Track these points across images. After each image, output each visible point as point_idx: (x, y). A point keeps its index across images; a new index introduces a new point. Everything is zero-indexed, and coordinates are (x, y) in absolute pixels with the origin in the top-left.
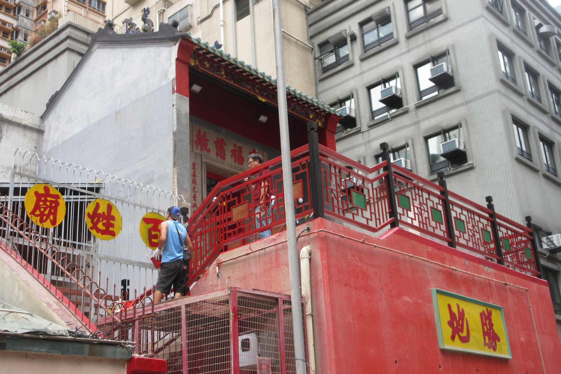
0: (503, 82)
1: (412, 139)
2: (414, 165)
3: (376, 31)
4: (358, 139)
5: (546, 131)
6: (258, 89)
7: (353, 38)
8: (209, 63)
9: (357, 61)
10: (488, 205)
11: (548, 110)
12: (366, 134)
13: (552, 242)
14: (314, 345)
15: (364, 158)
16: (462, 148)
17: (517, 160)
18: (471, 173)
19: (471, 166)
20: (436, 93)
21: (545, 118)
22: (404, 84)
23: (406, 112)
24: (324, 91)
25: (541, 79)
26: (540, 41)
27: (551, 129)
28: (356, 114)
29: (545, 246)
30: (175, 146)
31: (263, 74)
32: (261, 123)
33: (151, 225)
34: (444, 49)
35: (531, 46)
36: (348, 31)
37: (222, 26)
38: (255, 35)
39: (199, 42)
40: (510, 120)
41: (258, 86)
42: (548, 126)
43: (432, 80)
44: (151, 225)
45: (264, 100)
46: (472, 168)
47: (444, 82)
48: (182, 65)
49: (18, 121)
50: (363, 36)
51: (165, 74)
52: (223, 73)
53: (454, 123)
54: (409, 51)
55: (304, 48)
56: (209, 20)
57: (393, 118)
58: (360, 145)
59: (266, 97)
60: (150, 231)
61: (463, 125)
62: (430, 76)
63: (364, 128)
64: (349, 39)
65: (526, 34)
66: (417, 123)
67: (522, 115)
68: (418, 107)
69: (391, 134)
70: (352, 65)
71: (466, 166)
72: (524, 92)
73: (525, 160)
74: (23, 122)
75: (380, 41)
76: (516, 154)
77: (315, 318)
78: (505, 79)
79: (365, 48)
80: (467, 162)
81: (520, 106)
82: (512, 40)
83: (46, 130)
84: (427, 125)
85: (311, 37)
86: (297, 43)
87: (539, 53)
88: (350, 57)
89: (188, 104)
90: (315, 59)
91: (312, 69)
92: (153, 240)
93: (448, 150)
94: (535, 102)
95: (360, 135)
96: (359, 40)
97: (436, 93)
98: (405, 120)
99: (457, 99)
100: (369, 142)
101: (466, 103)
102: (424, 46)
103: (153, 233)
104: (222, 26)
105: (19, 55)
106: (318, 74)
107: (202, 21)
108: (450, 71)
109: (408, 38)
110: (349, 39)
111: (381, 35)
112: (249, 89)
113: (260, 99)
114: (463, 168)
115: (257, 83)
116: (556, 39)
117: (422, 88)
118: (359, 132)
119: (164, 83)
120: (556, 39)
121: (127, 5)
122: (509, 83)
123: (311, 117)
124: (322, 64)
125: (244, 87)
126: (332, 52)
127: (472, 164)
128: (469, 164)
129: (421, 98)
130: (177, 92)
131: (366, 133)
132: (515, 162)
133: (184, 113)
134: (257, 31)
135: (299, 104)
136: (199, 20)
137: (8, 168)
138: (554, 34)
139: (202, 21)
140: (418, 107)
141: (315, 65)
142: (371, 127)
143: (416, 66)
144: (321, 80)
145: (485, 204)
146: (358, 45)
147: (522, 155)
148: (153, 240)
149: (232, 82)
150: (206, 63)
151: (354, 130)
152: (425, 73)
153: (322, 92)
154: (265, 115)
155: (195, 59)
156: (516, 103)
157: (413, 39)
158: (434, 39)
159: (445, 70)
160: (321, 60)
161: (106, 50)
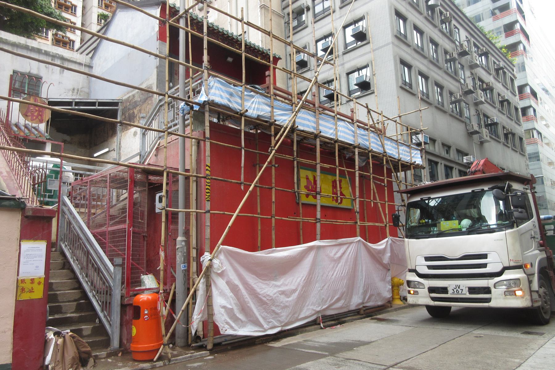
0: (396, 36)
3: (322, 4)
5: (424, 69)
7: (308, 9)
9: (310, 25)
11: (427, 56)
13: (418, 139)
14: (197, 200)
16: (368, 80)
17: (401, 87)
18: (373, 95)
20: (355, 45)
21: (425, 62)
25: (425, 35)
26: (428, 10)
27: (428, 68)
29: (414, 141)
30: (158, 75)
31: (223, 29)
32: (229, 62)
34: (362, 16)
35: (421, 13)
36: (305, 4)
38: (248, 7)
39: (175, 6)
40: (398, 62)
41: (220, 37)
42: (426, 66)
43: (352, 36)
46: (373, 93)
47: (361, 37)
49: (75, 60)
50: (314, 7)
51: (153, 28)
53: (364, 64)
54: (341, 17)
55: (279, 15)
61: (370, 65)
62: (352, 34)
64: (305, 10)
65: (418, 6)
66: (343, 64)
67: (408, 59)
68: (344, 54)
69: (325, 72)
70: (307, 27)
71: (369, 92)
72: (411, 44)
73: (407, 88)
74: (78, 61)
75: (324, 10)
76: (400, 84)
77: (199, 183)
78: (399, 36)
79: (315, 16)
81: (407, 53)
82: (406, 9)
83: (94, 66)
84: (349, 66)
85: (284, 9)
86: (273, 12)
87: (426, 18)
88: (306, 22)
90: (285, 23)
91: (284, 29)
93: (359, 81)
94: (419, 51)
95: (310, 72)
96: (311, 10)
97: (355, 45)
99: (367, 48)
102: (348, 14)
105: (105, 21)
108: (364, 30)
109: (341, 8)
110: (305, 10)
111: (326, 7)
114: (368, 93)
115: (220, 35)
116: (439, 9)
117: (347, 42)
118: (309, 70)
119: (153, 34)
120: (439, 9)
122: (401, 39)
129: (347, 48)
130: (160, 39)
132: (400, 89)
134: (249, 4)
135: (251, 50)
137: (69, 90)
138: (438, 6)
141: (285, 27)
143: (345, 27)
146: (310, 13)
147: (405, 85)
151: (305, 69)
152: (349, 31)
154: (231, 57)
156: (404, 51)
157: (344, 9)
158: (356, 9)
159: (361, 29)
161: (123, 13)
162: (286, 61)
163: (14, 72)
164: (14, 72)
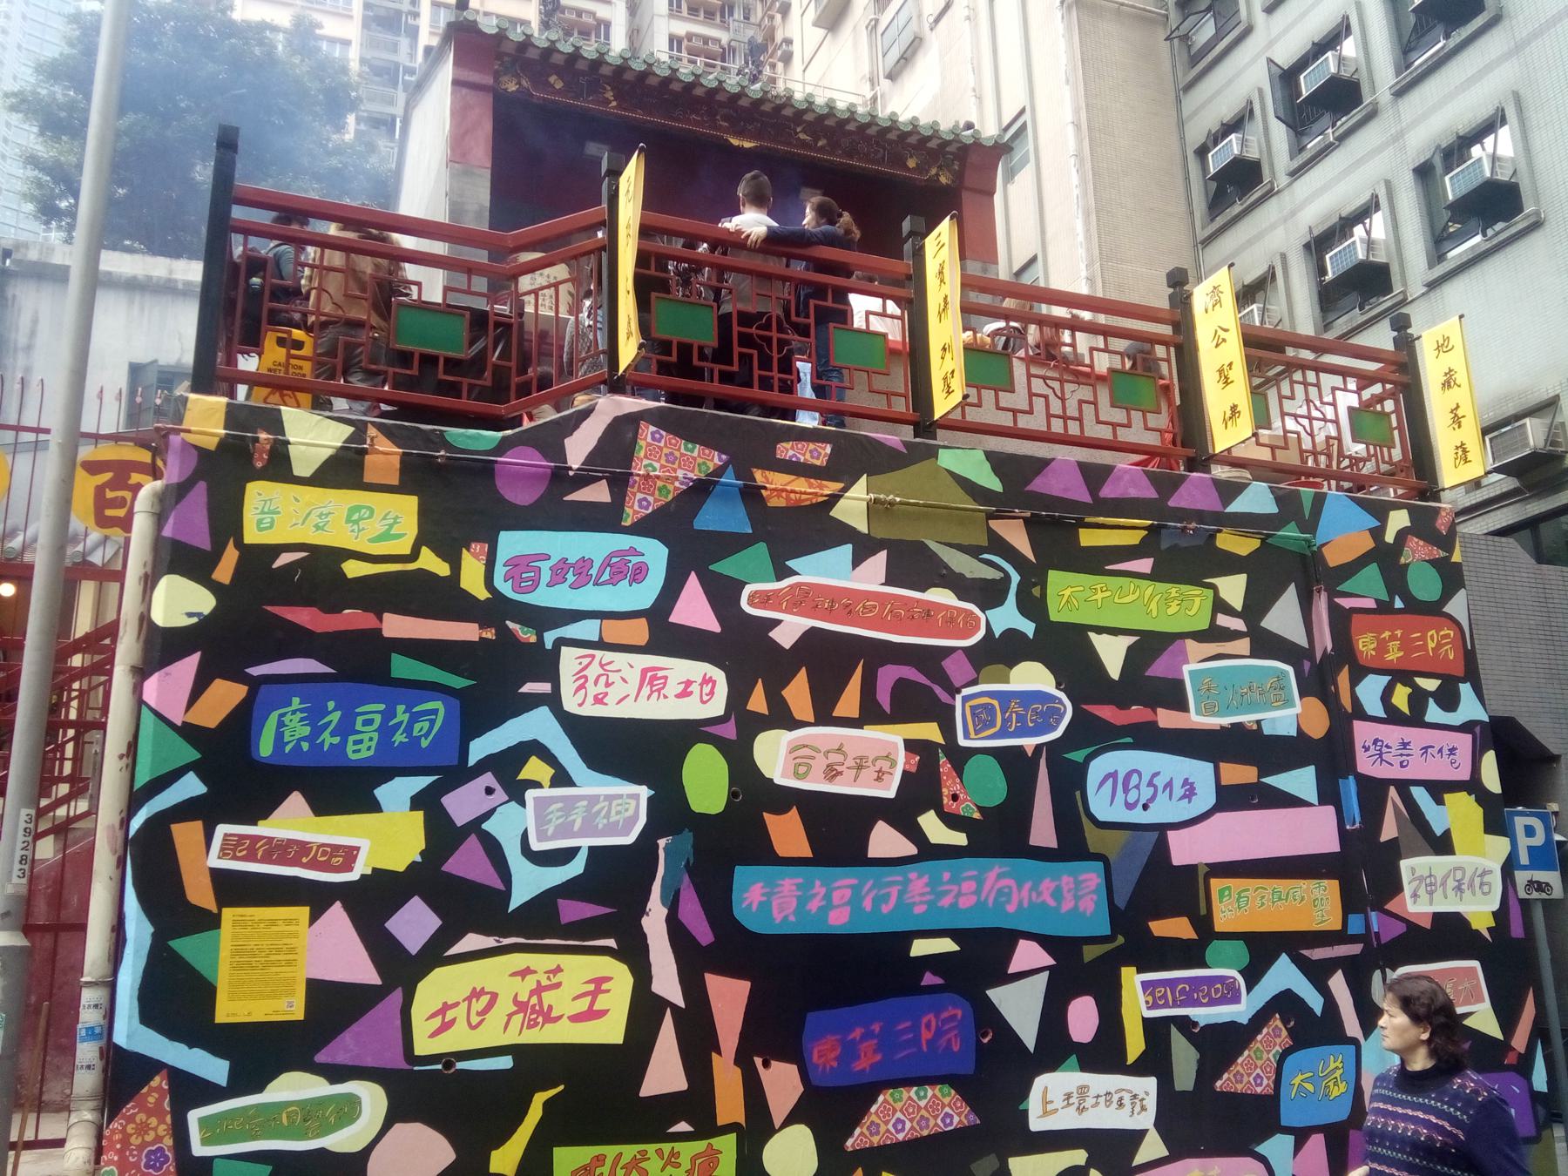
1: (1388, 184)
2: (1393, 247)
4: (1270, 212)
6: (725, 118)
8: (561, 77)
10: (1171, 297)
12: (1285, 196)
15: (1284, 257)
16: (1504, 176)
18: (1536, 238)
19: (1532, 220)
22: (1365, 45)
23: (1372, 115)
24: (1195, 113)
28: (1261, 152)
33: (107, 476)
37: (968, 18)
44: (107, 476)
45: (747, 145)
46: (1536, 225)
48: (464, 91)
52: (609, 95)
53: (1484, 112)
56: (950, 12)
57: (1342, 138)
58: (1273, 227)
59: (751, 138)
60: (100, 491)
61: (1511, 114)
63: (1282, 180)
66: (1399, 136)
70: (1248, 31)
71: (1520, 223)
80: (1521, 210)
89: (488, 184)
92: (109, 512)
95: (1274, 201)
98: (1369, 137)
99: (1492, 45)
100: (1293, 213)
101: (1518, 48)
103: (110, 494)
104: (968, 18)
106: (1180, 74)
107: (937, 21)
112: (697, 123)
113: (735, 142)
114: (1513, 230)
115: (721, 104)
118: (1270, 194)
121: (821, 32)
123: (911, 163)
124: (1189, 47)
125: (678, 120)
126: (1208, 10)
127: (1537, 213)
128: (1528, 216)
131: (1286, 193)
133: (472, 207)
136: (931, 19)
139: (937, 21)
140: (1400, 93)
142: (1295, 174)
144: (1189, 87)
145: (1160, 298)
148: (109, 512)
149: (638, 115)
150: (552, 79)
153: (1191, 117)
155: (517, 76)
160: (1185, 38)
162: (1187, 178)
163: (135, 370)
164: (135, 370)
